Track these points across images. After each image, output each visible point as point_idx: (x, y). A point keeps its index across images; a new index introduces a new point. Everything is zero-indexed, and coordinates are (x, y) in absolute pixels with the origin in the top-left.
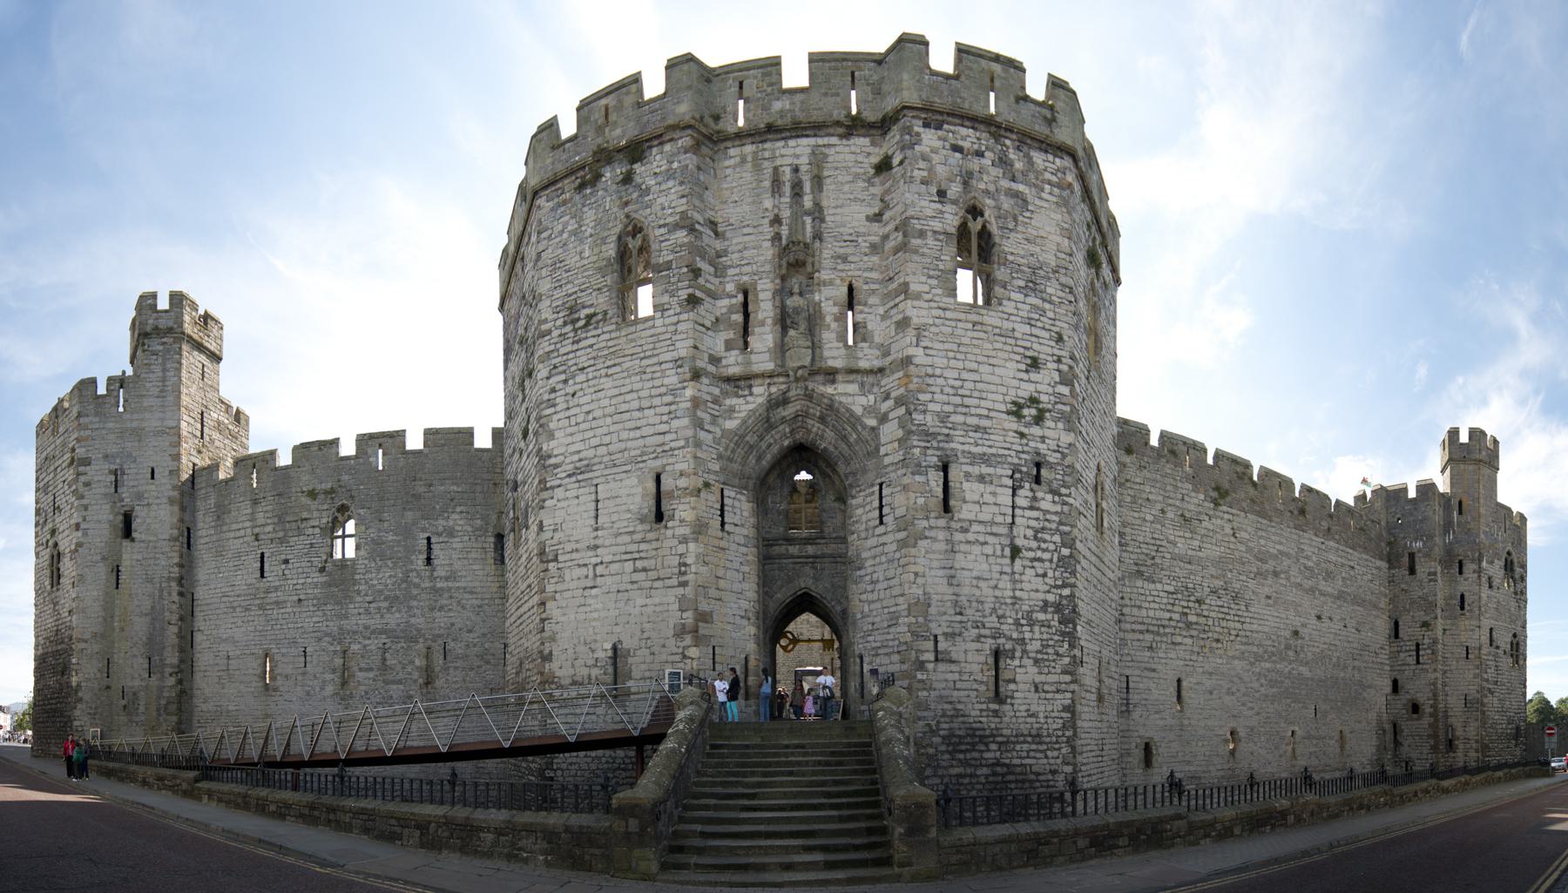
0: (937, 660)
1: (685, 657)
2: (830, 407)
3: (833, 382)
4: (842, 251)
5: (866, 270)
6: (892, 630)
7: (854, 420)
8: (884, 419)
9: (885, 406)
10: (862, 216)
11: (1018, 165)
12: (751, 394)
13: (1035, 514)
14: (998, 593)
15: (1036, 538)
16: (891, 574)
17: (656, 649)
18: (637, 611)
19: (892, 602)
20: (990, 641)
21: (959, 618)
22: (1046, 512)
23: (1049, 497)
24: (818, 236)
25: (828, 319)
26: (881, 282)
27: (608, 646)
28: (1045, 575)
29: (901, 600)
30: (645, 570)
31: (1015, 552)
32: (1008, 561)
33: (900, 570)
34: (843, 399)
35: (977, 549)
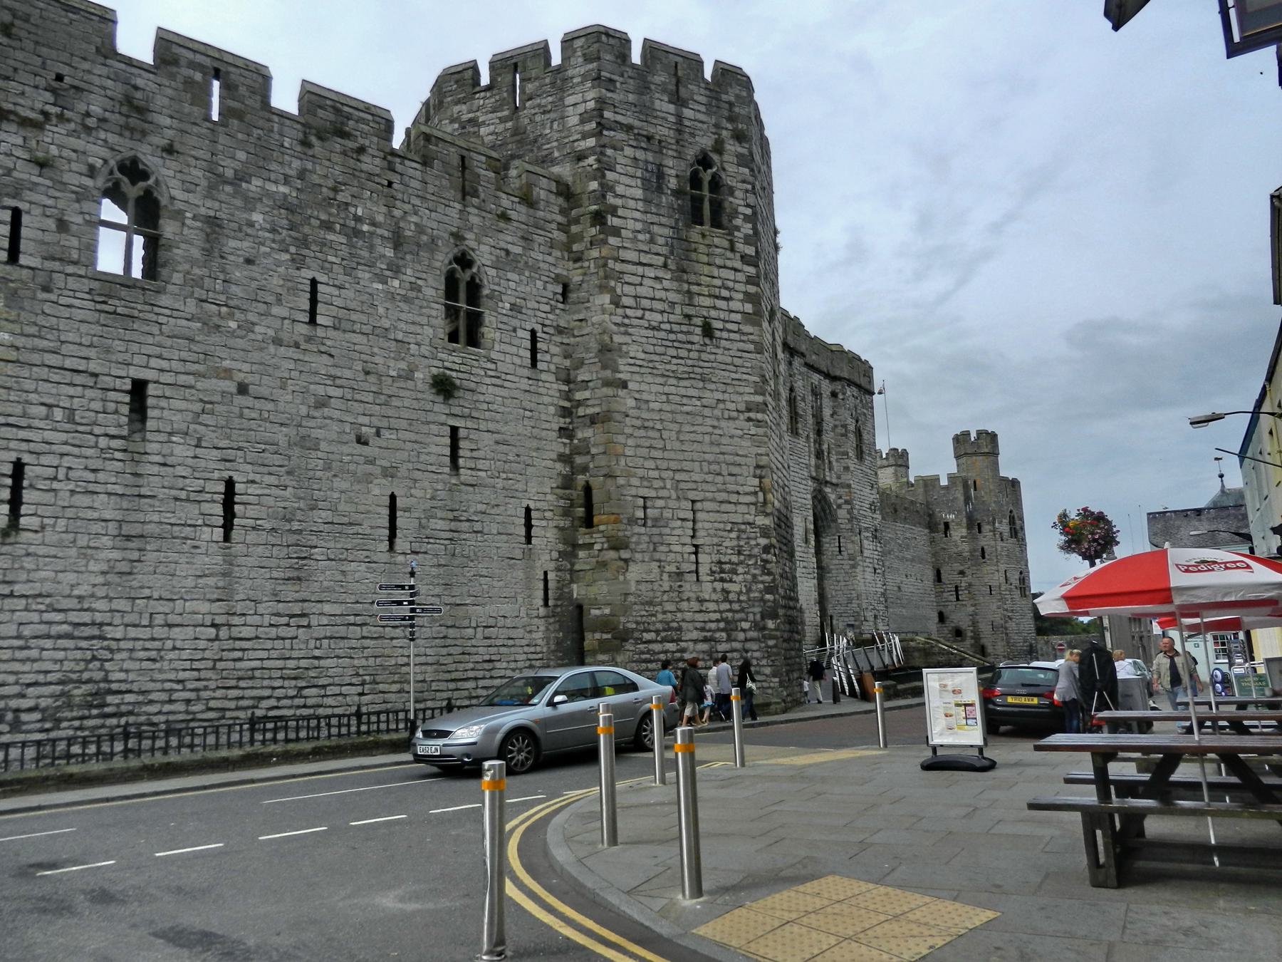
7: (830, 506)
8: (839, 506)
9: (840, 501)
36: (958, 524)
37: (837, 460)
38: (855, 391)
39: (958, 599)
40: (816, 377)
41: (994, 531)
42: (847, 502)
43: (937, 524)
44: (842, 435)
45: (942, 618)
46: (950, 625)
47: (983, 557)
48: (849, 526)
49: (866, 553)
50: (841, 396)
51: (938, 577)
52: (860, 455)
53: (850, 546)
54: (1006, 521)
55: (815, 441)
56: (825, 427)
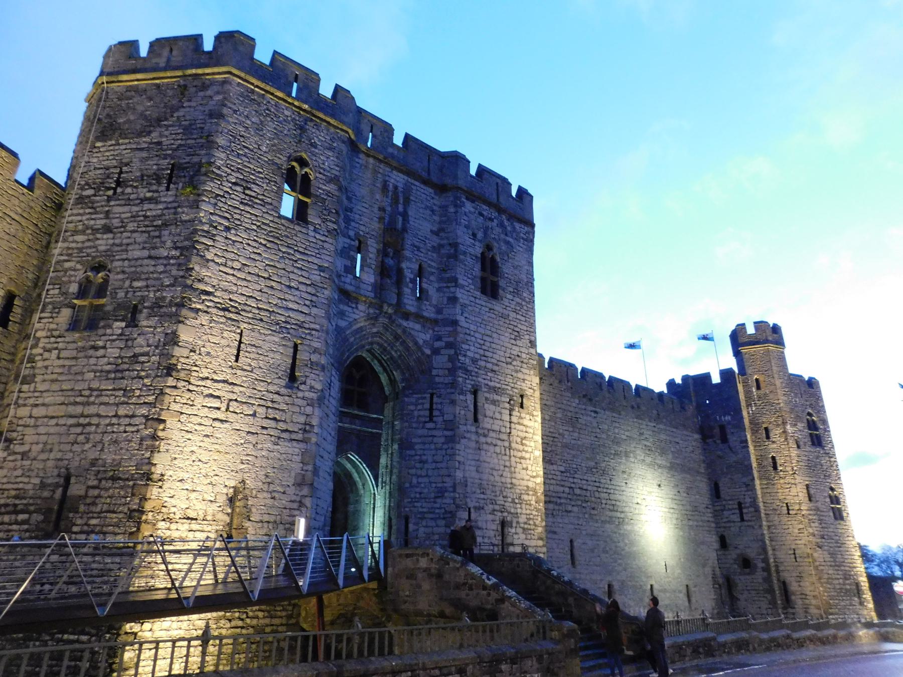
3: (407, 319)
4: (417, 244)
5: (429, 260)
6: (439, 500)
8: (436, 352)
9: (438, 344)
12: (357, 308)
16: (438, 458)
19: (439, 479)
20: (500, 514)
21: (482, 496)
24: (404, 230)
37: (439, 290)
39: (742, 520)
42: (449, 345)
46: (733, 554)
48: (448, 380)
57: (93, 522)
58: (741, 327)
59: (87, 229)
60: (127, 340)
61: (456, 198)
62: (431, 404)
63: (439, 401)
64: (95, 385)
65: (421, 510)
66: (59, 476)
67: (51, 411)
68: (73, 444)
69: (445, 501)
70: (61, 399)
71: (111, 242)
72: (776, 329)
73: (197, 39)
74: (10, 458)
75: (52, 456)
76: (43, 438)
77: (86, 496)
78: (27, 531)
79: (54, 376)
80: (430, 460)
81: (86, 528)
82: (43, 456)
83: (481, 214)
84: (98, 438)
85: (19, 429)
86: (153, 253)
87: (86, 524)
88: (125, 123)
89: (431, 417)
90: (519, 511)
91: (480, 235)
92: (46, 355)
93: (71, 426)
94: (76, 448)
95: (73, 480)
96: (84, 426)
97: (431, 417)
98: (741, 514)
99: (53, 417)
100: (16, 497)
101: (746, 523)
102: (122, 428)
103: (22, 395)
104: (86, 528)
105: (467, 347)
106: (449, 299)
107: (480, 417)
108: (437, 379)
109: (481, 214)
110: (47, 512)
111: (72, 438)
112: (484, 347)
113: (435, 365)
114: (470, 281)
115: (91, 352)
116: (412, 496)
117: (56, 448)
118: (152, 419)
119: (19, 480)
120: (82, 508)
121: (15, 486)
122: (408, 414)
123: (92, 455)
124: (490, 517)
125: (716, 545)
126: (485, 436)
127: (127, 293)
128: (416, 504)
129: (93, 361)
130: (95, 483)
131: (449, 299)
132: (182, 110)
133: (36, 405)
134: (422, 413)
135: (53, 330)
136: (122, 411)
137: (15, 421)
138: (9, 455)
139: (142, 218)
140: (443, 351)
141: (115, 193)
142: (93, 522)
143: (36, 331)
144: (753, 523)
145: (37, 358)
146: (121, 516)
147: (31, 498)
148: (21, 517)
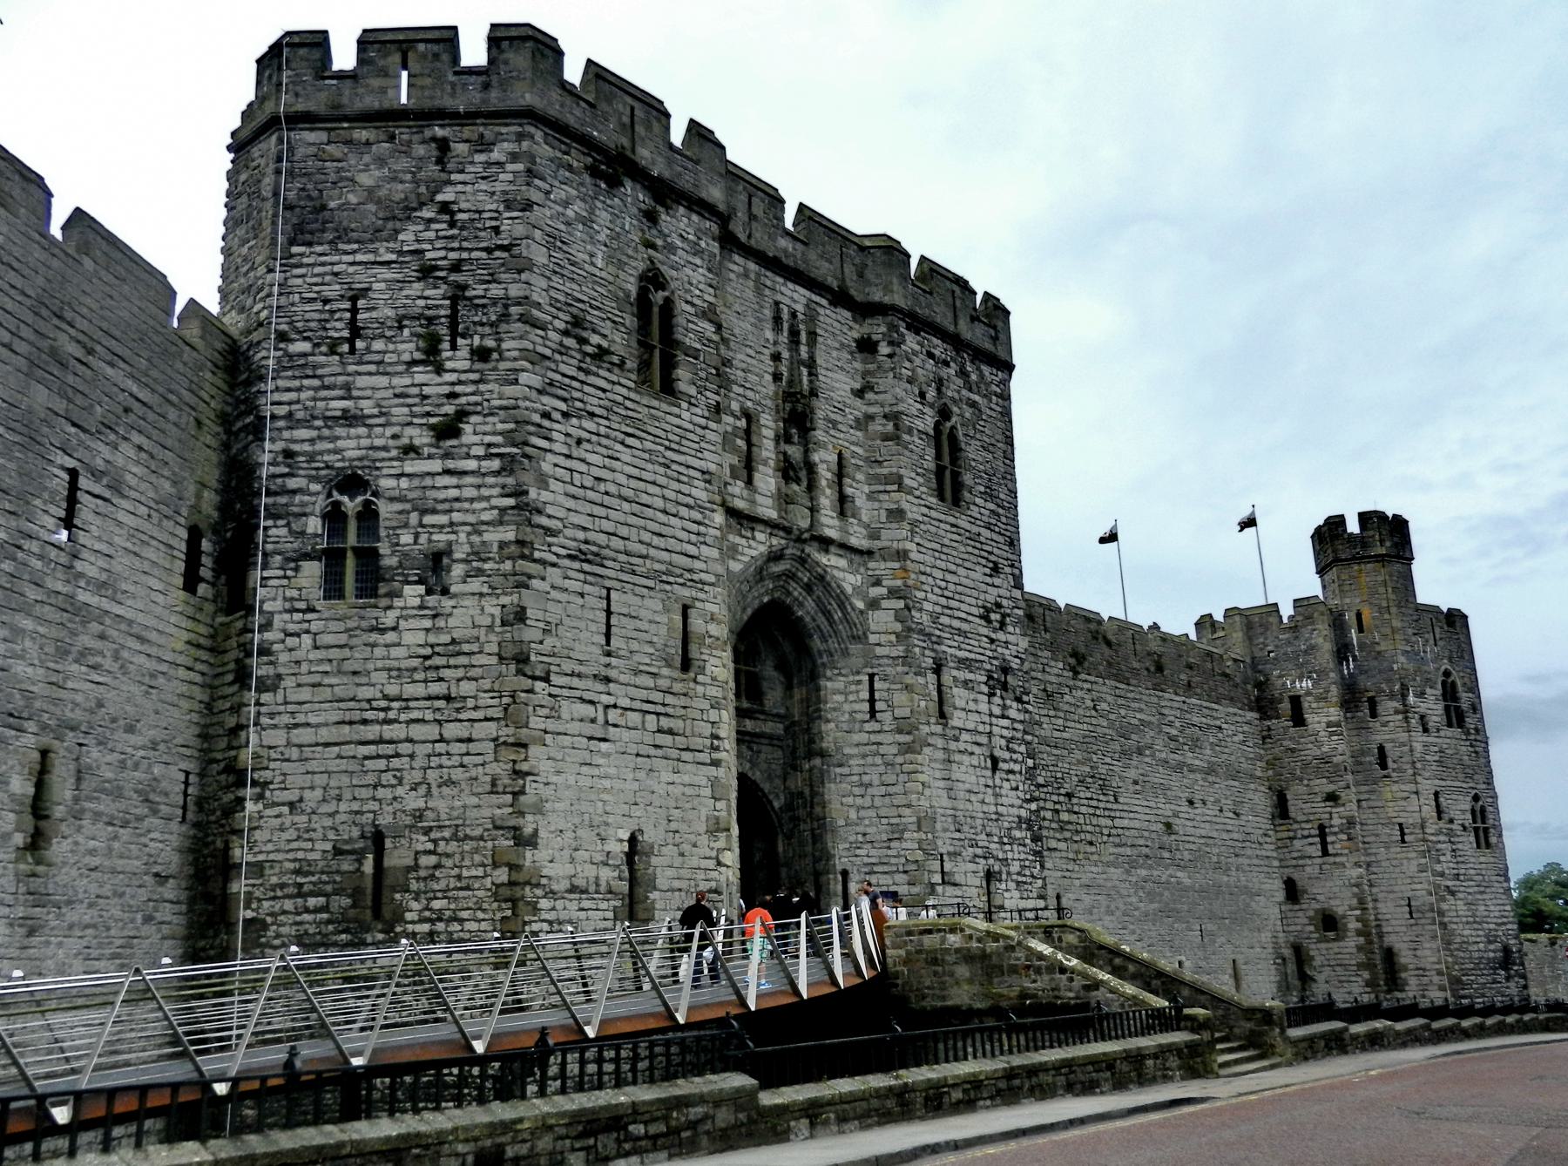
0: (944, 882)
1: (719, 864)
2: (822, 578)
3: (827, 551)
4: (833, 416)
5: (852, 443)
7: (842, 601)
8: (874, 604)
9: (875, 592)
10: (848, 388)
11: (974, 377)
13: (1005, 722)
14: (985, 808)
15: (1008, 749)
16: (891, 779)
17: (686, 847)
18: (661, 789)
19: (894, 812)
20: (982, 861)
21: (957, 835)
22: (1014, 720)
23: (1015, 705)
24: (814, 393)
25: (824, 483)
26: (867, 460)
27: (626, 836)
28: (1017, 789)
29: (907, 811)
30: (670, 732)
31: (995, 761)
32: (989, 773)
33: (903, 778)
34: (835, 572)
35: (966, 758)
36: (1319, 699)
37: (871, 496)
38: (939, 348)
39: (1325, 853)
40: (796, 297)
41: (1406, 711)
42: (893, 593)
43: (1274, 702)
44: (886, 438)
45: (1293, 892)
46: (1310, 907)
47: (1384, 766)
48: (899, 651)
49: (957, 719)
50: (884, 349)
51: (1281, 809)
52: (949, 486)
53: (900, 698)
54: (1434, 693)
55: (783, 438)
56: (822, 410)
57: (436, 904)
58: (1335, 524)
59: (314, 418)
60: (435, 616)
61: (893, 327)
62: (872, 691)
63: (886, 686)
64: (392, 690)
65: (866, 860)
66: (363, 836)
67: (325, 734)
68: (375, 787)
69: (905, 845)
70: (335, 716)
71: (365, 442)
72: (1396, 529)
73: (447, 38)
74: (268, 812)
75: (343, 807)
76: (320, 780)
77: (416, 867)
78: (329, 922)
79: (316, 678)
80: (876, 782)
81: (427, 914)
82: (325, 808)
83: (930, 355)
84: (417, 776)
85: (272, 765)
86: (451, 464)
87: (427, 908)
88: (339, 208)
89: (873, 712)
90: (1010, 855)
91: (931, 394)
92: (291, 642)
93: (366, 758)
94: (381, 793)
95: (388, 843)
96: (388, 757)
97: (873, 712)
98: (1324, 844)
99: (327, 745)
100: (297, 872)
101: (1331, 859)
102: (456, 760)
103: (263, 709)
104: (427, 914)
105: (920, 595)
106: (890, 512)
107: (946, 708)
108: (879, 651)
109: (930, 355)
110: (356, 894)
111: (370, 779)
112: (946, 593)
113: (873, 628)
114: (921, 480)
115: (374, 637)
116: (852, 839)
117: (347, 795)
118: (505, 743)
119: (295, 845)
120: (414, 886)
121: (291, 856)
122: (835, 709)
123: (414, 802)
124: (972, 867)
125: (1280, 896)
126: (957, 740)
127: (417, 535)
128: (858, 852)
129: (379, 652)
130: (430, 846)
131: (890, 512)
132: (449, 189)
133: (296, 726)
134: (857, 707)
135: (292, 599)
136: (451, 730)
137: (264, 752)
138: (266, 807)
139: (417, 400)
140: (885, 604)
141: (353, 350)
142: (436, 904)
143: (262, 602)
144: (1343, 859)
145: (276, 647)
146: (481, 893)
147: (322, 873)
148: (312, 902)
